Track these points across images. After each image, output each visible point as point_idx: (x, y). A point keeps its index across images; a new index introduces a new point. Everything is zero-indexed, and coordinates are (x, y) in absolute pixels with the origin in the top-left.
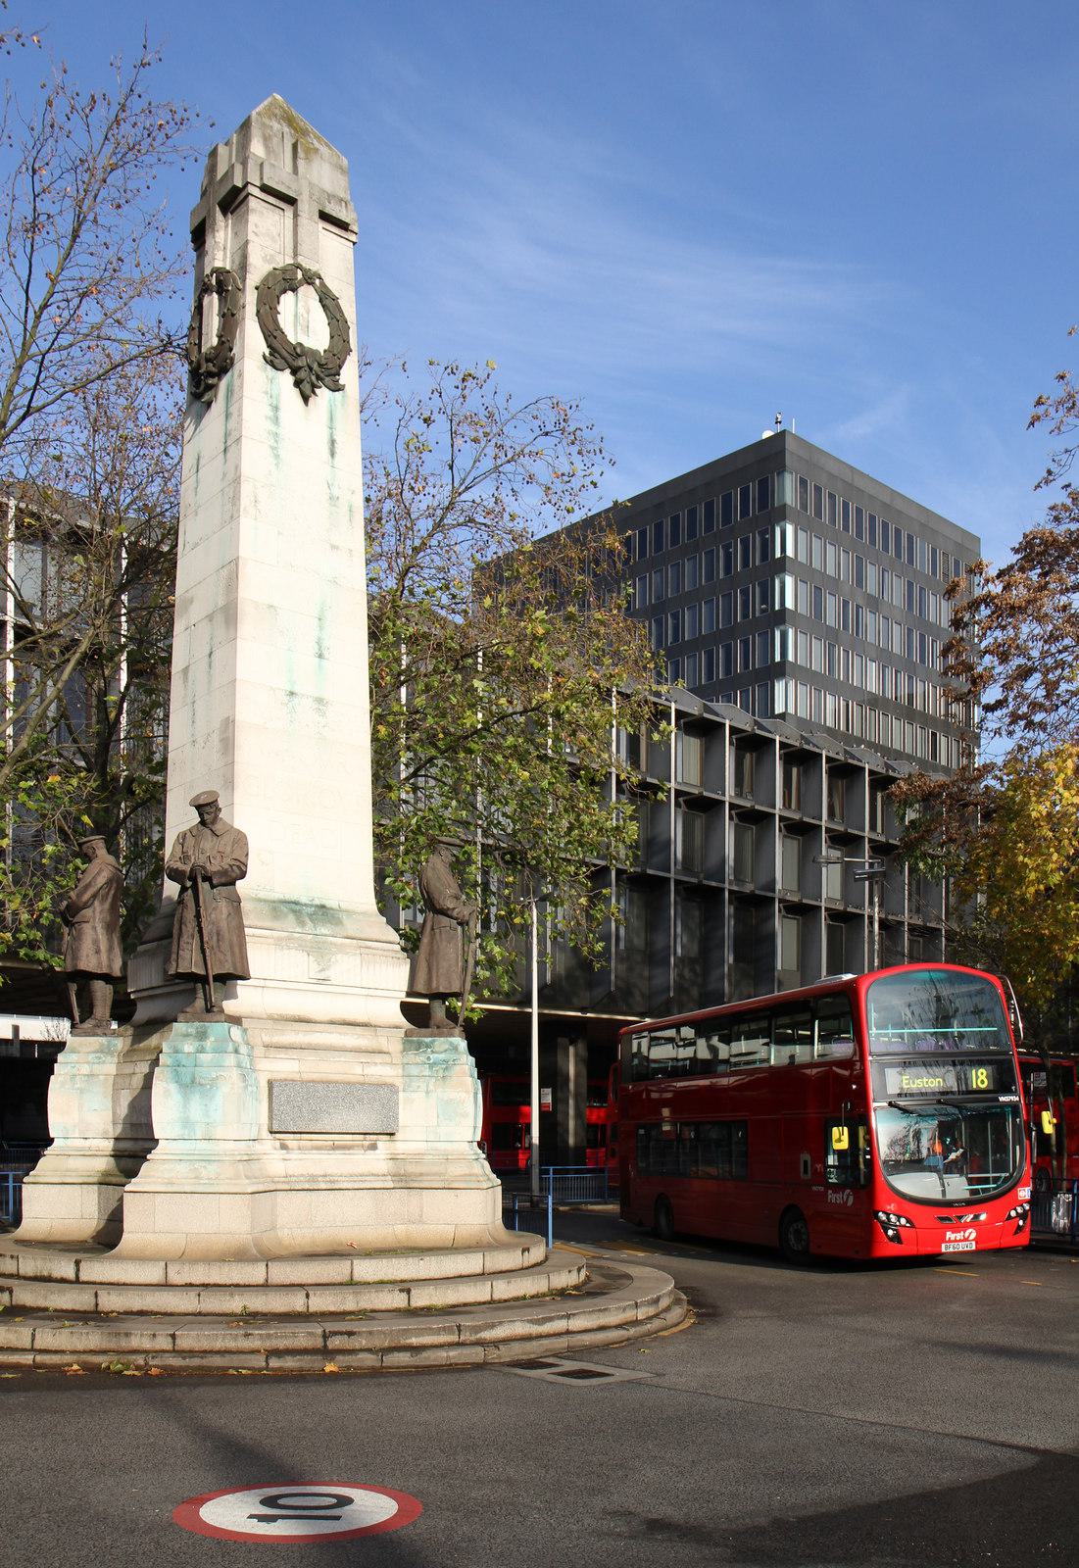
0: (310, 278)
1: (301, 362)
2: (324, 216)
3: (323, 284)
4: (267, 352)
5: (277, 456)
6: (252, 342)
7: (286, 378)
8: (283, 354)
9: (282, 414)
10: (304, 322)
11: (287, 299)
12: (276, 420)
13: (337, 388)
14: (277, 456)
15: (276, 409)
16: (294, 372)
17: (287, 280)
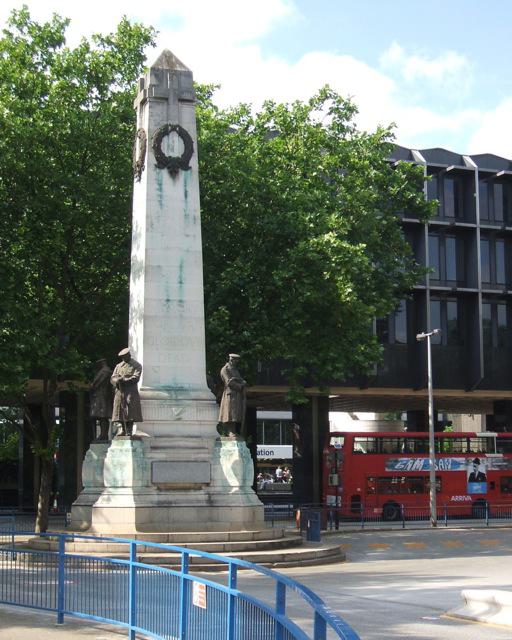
0: (174, 128)
1: (170, 165)
2: (182, 100)
3: (180, 128)
4: (156, 163)
5: (161, 205)
6: (150, 159)
7: (165, 173)
8: (163, 162)
9: (163, 187)
10: (174, 147)
11: (165, 139)
12: (161, 190)
13: (187, 168)
14: (161, 205)
15: (160, 185)
16: (169, 168)
17: (164, 132)
